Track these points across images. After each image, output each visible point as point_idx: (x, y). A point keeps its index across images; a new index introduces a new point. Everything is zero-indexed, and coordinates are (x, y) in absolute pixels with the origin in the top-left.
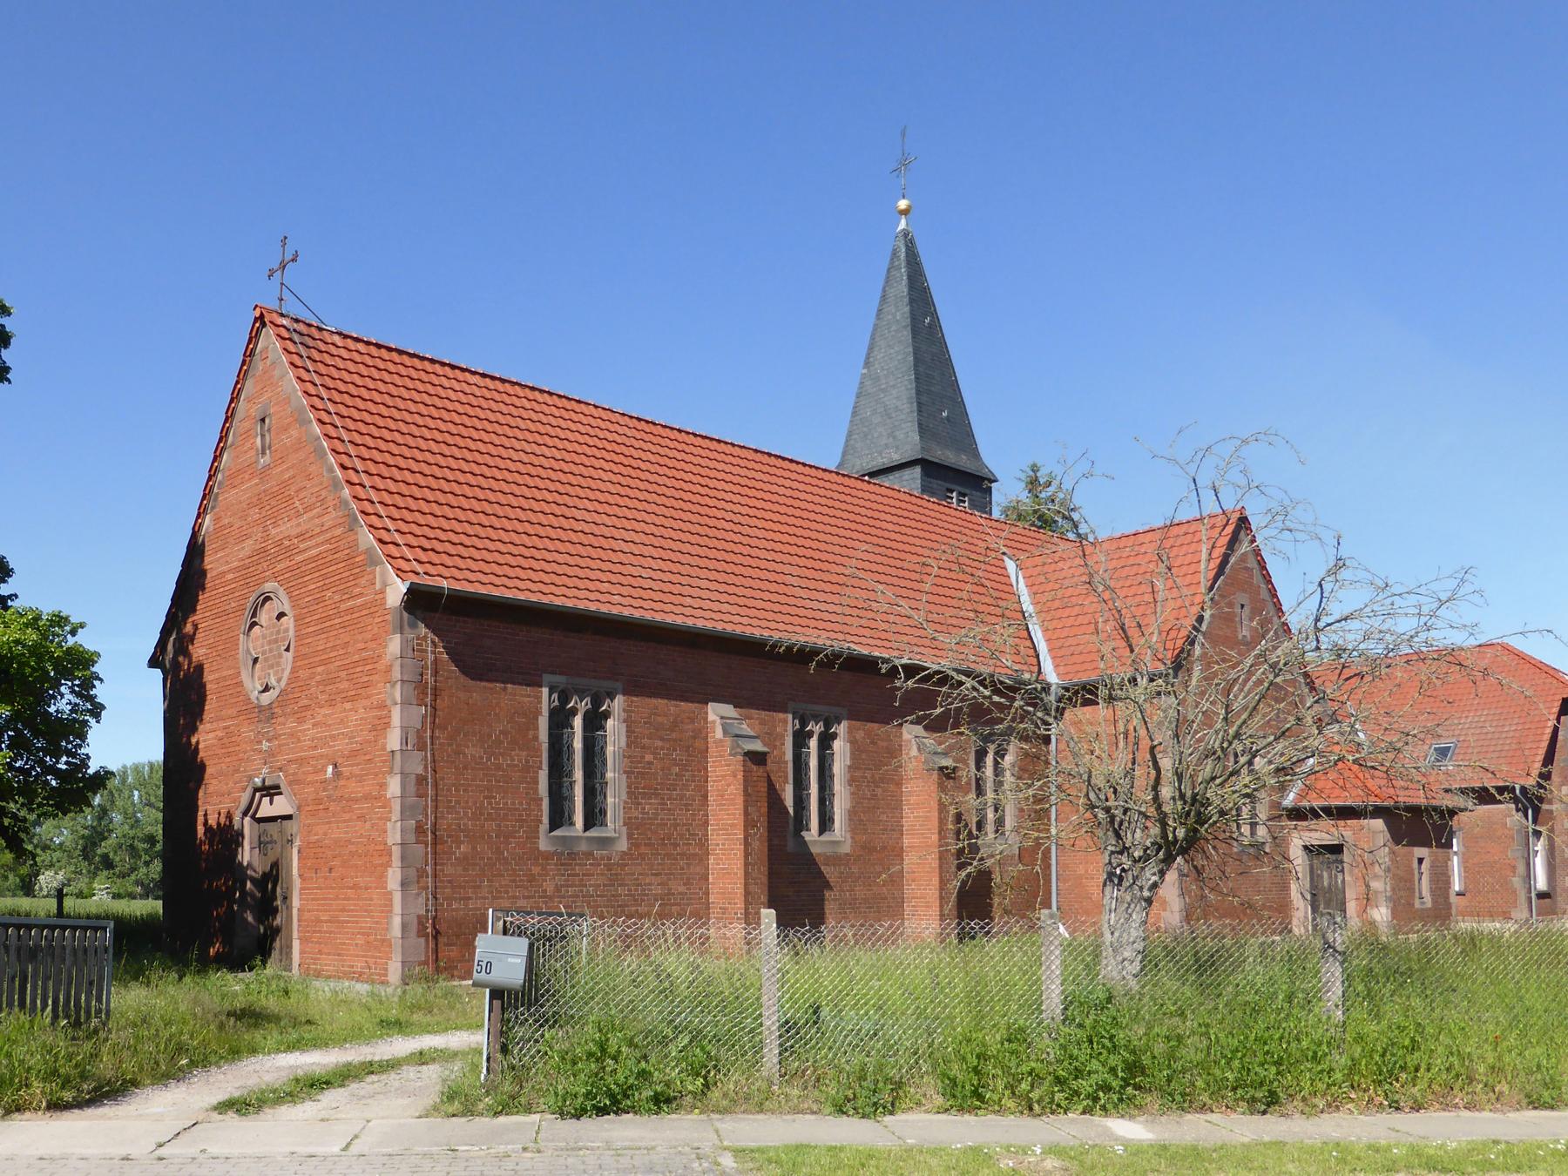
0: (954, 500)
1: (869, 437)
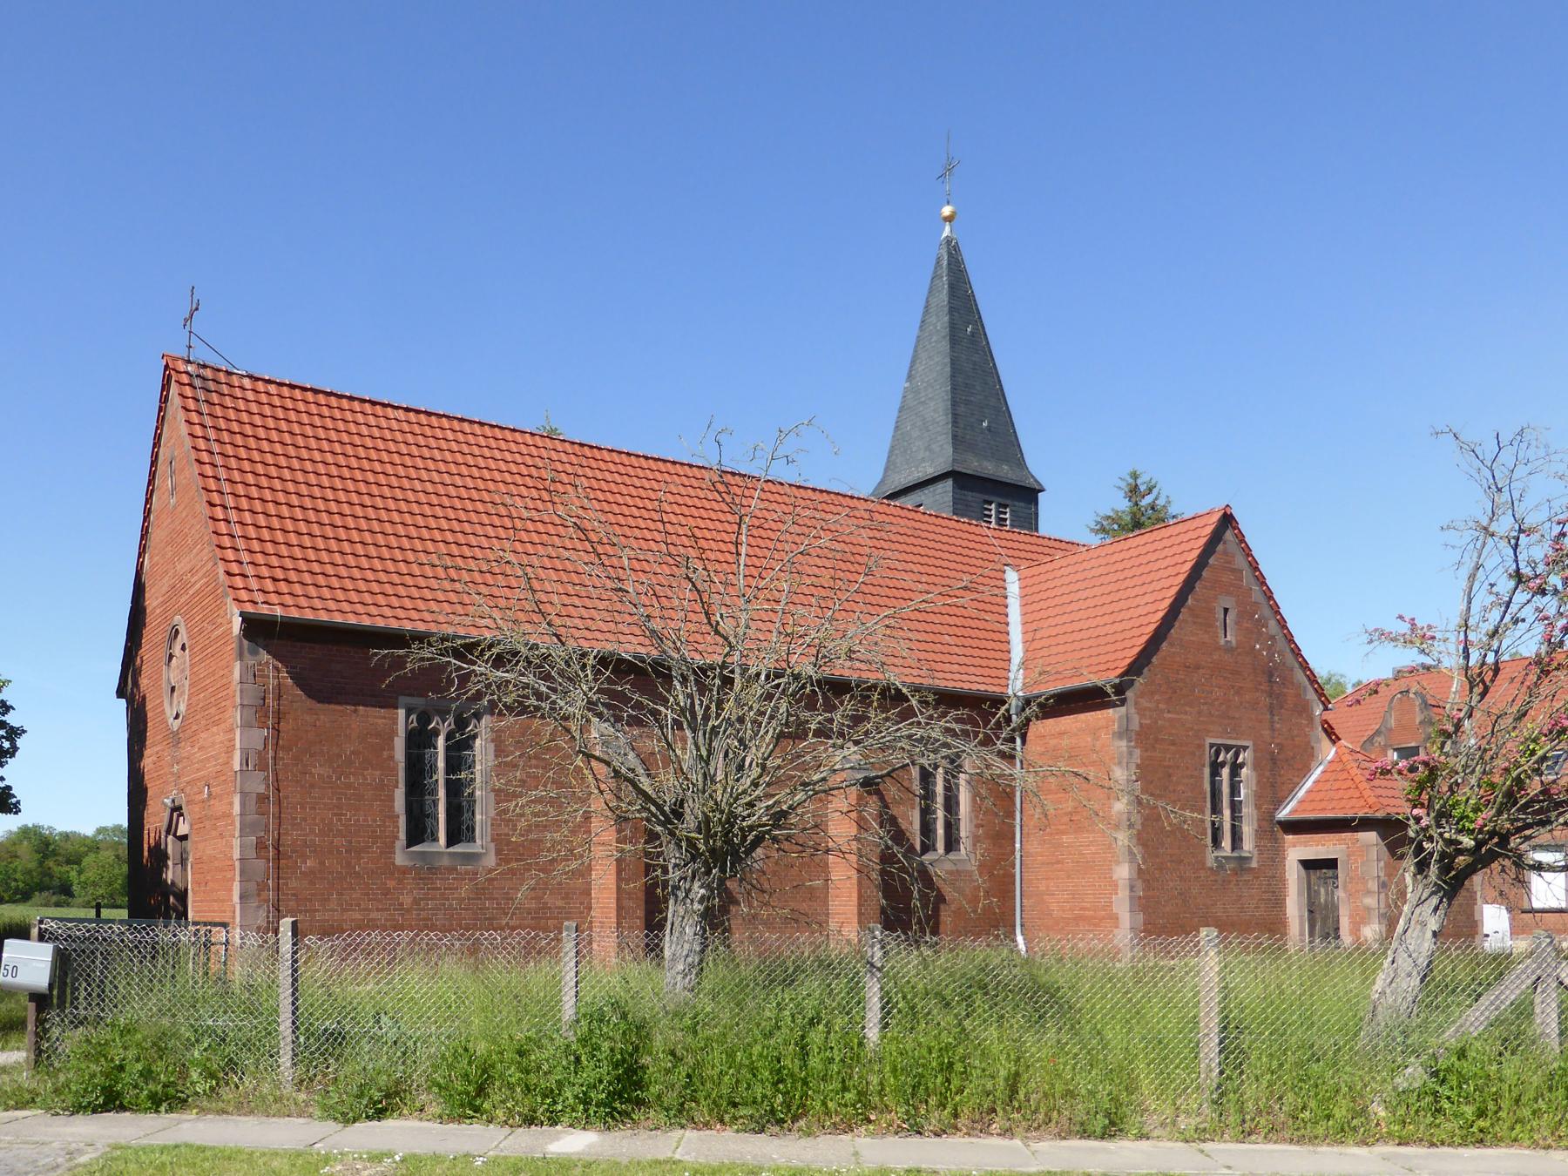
0: (993, 512)
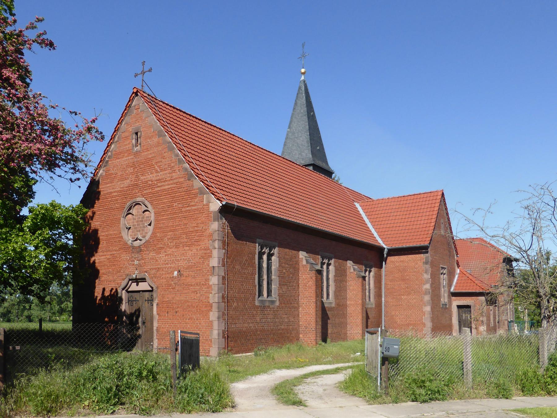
1: (291, 154)
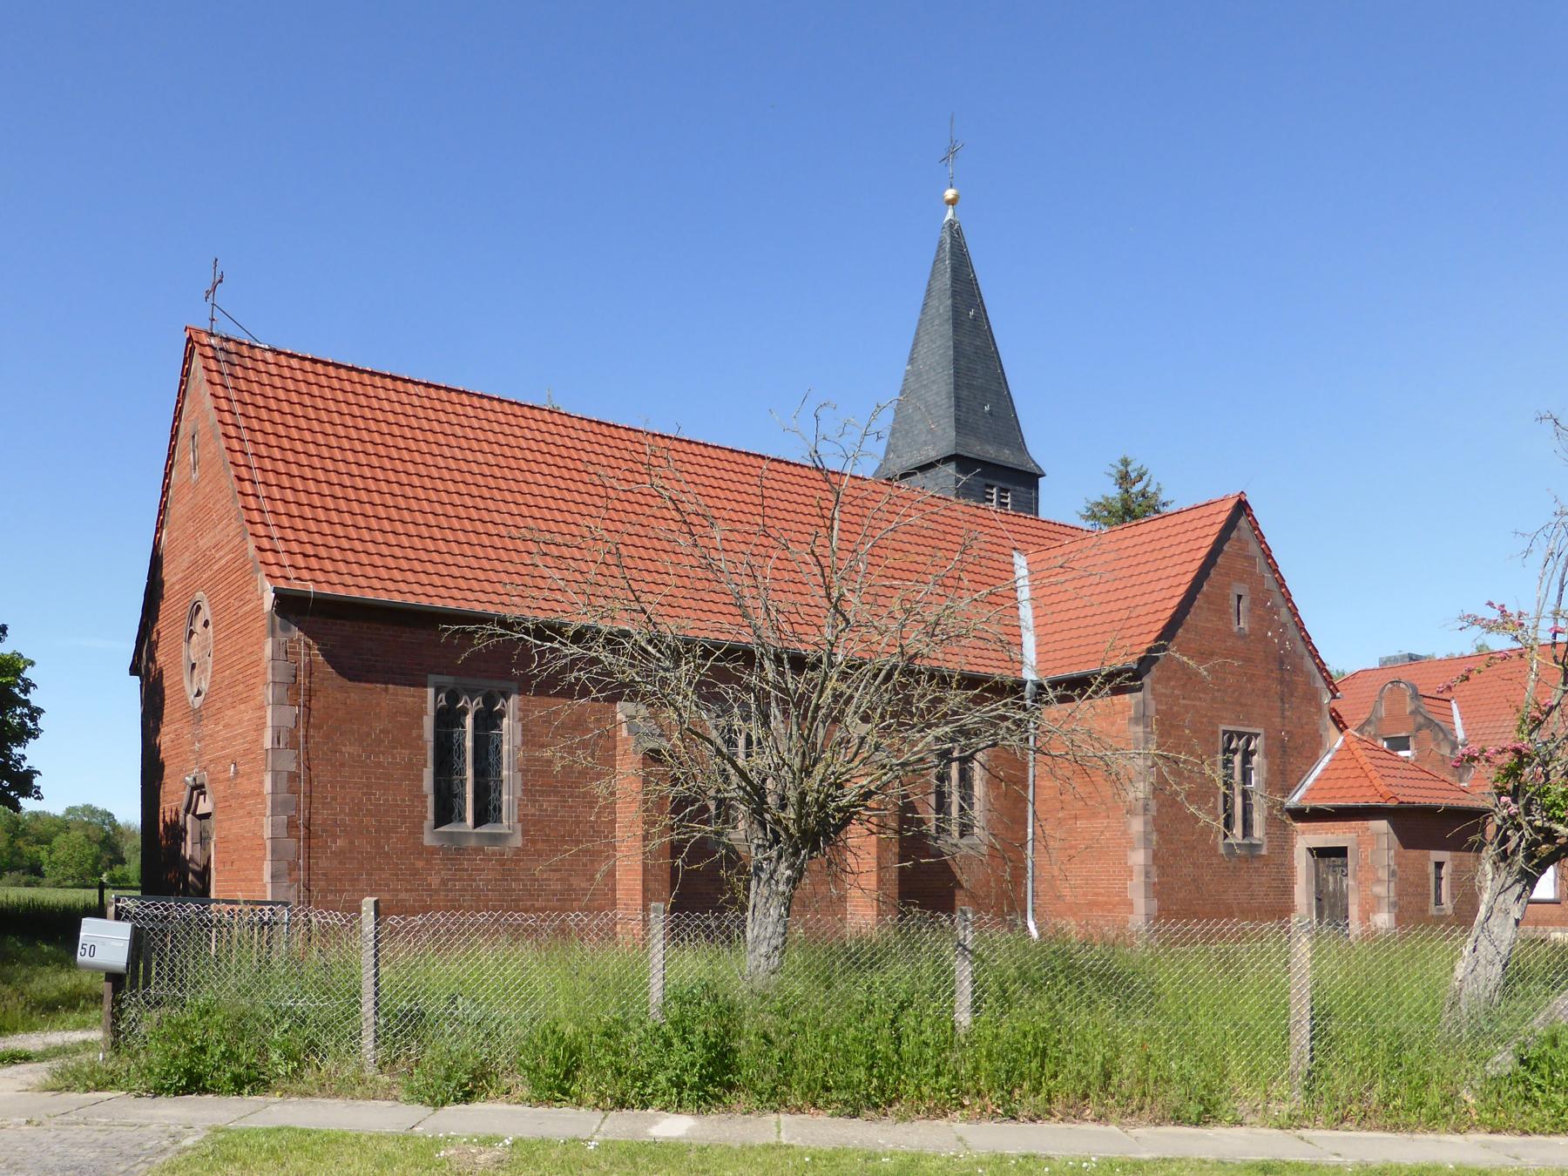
0: (994, 497)
1: (910, 435)
